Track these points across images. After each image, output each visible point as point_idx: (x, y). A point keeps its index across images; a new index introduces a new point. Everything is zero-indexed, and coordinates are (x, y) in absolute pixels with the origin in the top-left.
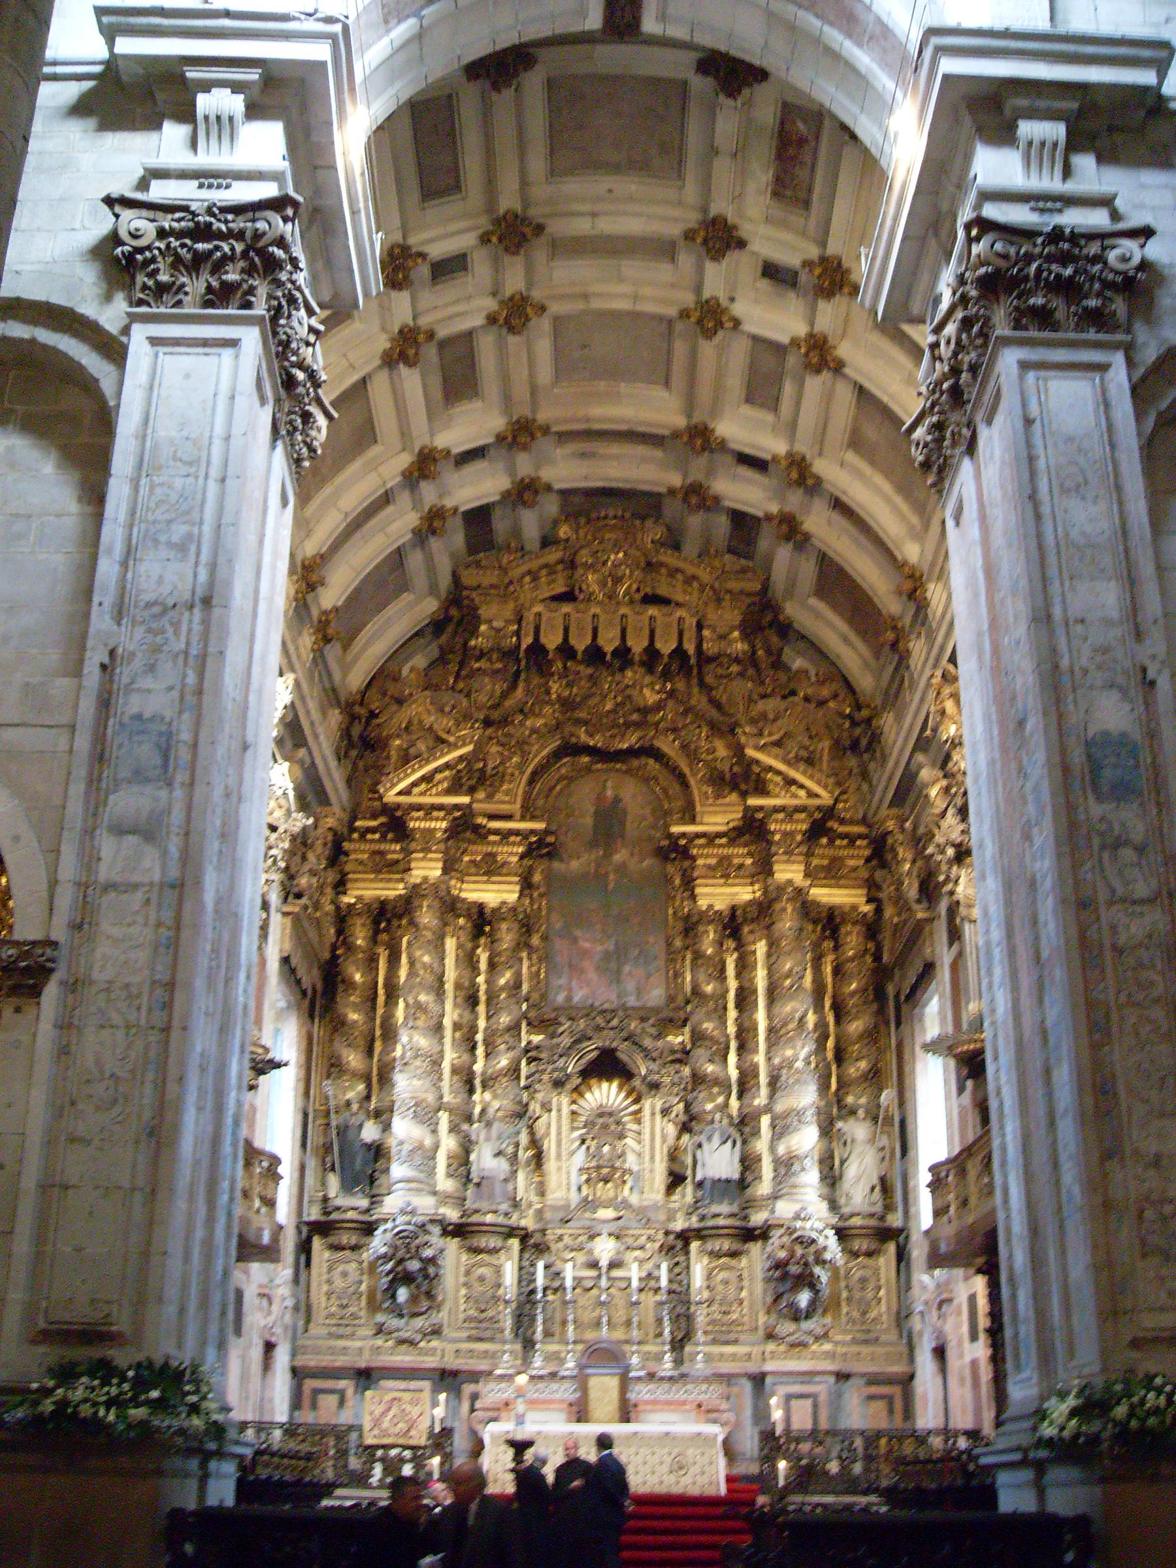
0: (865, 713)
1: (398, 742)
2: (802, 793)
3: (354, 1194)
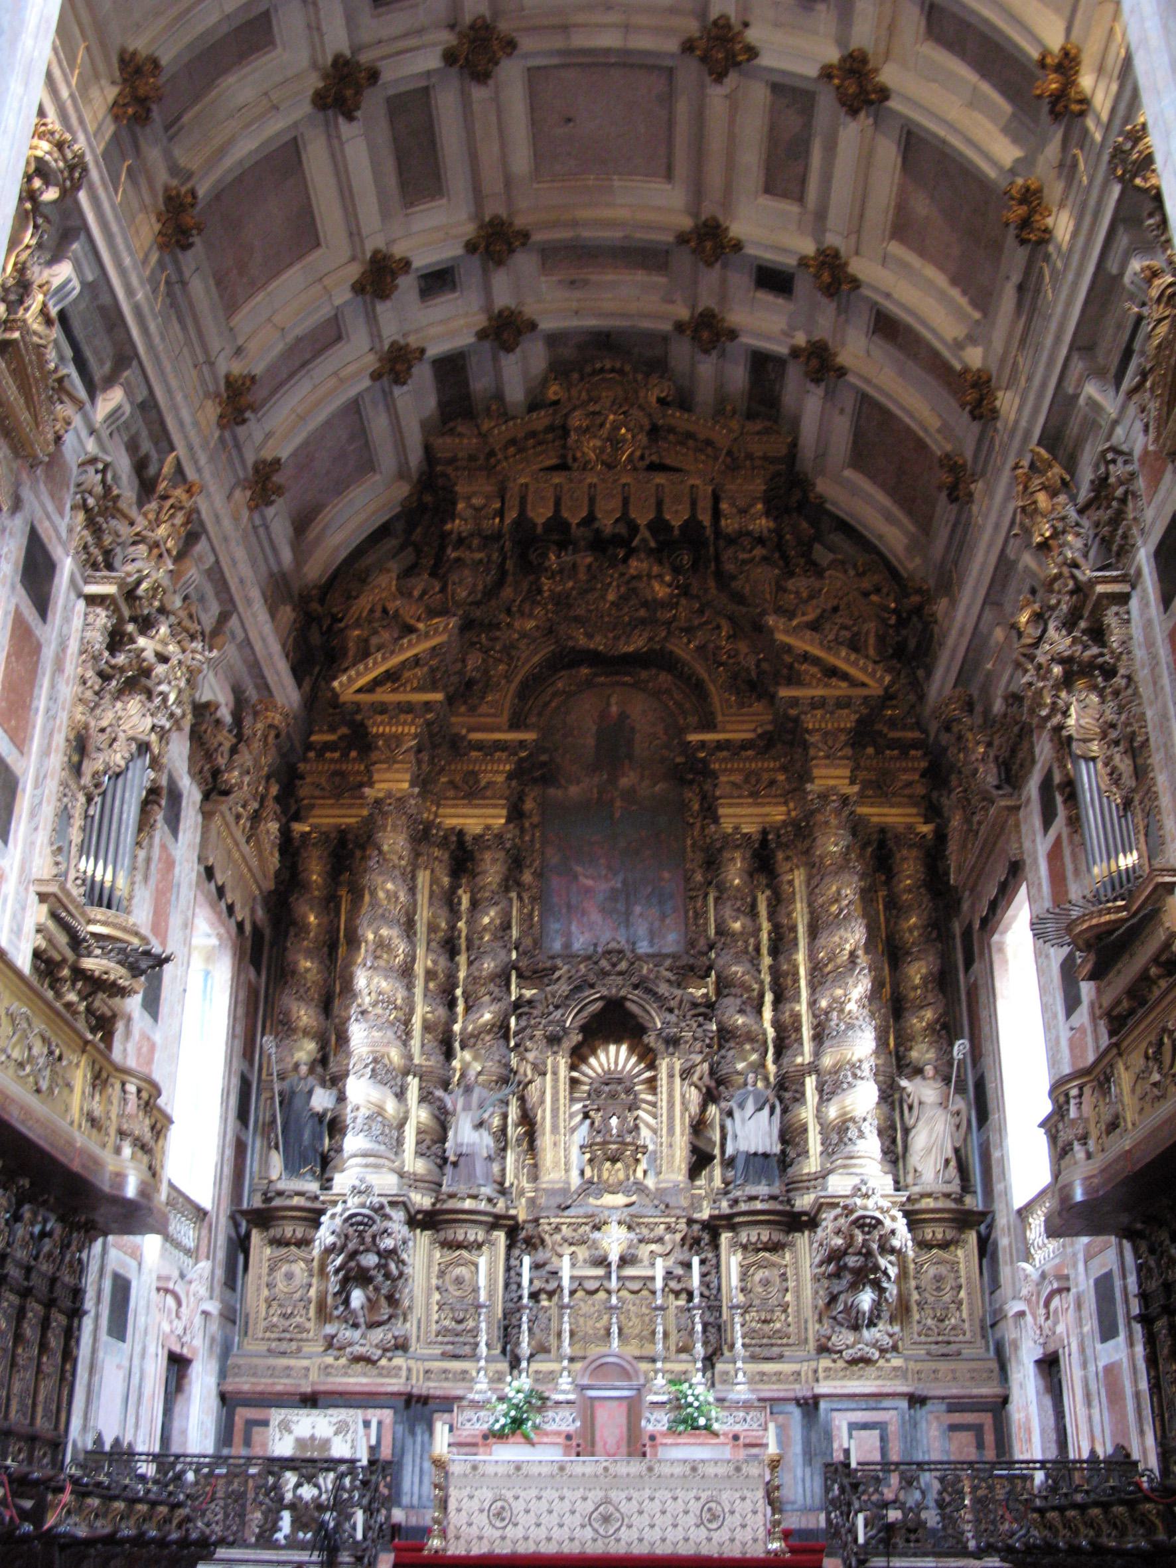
0: (915, 599)
1: (357, 633)
2: (844, 685)
3: (300, 1176)
